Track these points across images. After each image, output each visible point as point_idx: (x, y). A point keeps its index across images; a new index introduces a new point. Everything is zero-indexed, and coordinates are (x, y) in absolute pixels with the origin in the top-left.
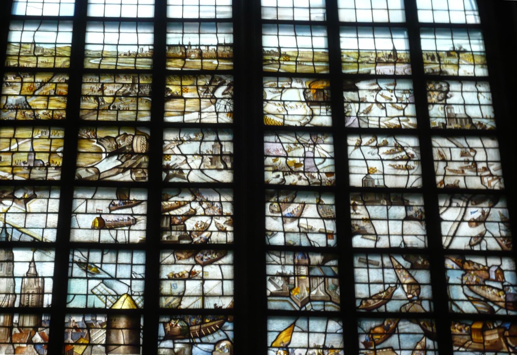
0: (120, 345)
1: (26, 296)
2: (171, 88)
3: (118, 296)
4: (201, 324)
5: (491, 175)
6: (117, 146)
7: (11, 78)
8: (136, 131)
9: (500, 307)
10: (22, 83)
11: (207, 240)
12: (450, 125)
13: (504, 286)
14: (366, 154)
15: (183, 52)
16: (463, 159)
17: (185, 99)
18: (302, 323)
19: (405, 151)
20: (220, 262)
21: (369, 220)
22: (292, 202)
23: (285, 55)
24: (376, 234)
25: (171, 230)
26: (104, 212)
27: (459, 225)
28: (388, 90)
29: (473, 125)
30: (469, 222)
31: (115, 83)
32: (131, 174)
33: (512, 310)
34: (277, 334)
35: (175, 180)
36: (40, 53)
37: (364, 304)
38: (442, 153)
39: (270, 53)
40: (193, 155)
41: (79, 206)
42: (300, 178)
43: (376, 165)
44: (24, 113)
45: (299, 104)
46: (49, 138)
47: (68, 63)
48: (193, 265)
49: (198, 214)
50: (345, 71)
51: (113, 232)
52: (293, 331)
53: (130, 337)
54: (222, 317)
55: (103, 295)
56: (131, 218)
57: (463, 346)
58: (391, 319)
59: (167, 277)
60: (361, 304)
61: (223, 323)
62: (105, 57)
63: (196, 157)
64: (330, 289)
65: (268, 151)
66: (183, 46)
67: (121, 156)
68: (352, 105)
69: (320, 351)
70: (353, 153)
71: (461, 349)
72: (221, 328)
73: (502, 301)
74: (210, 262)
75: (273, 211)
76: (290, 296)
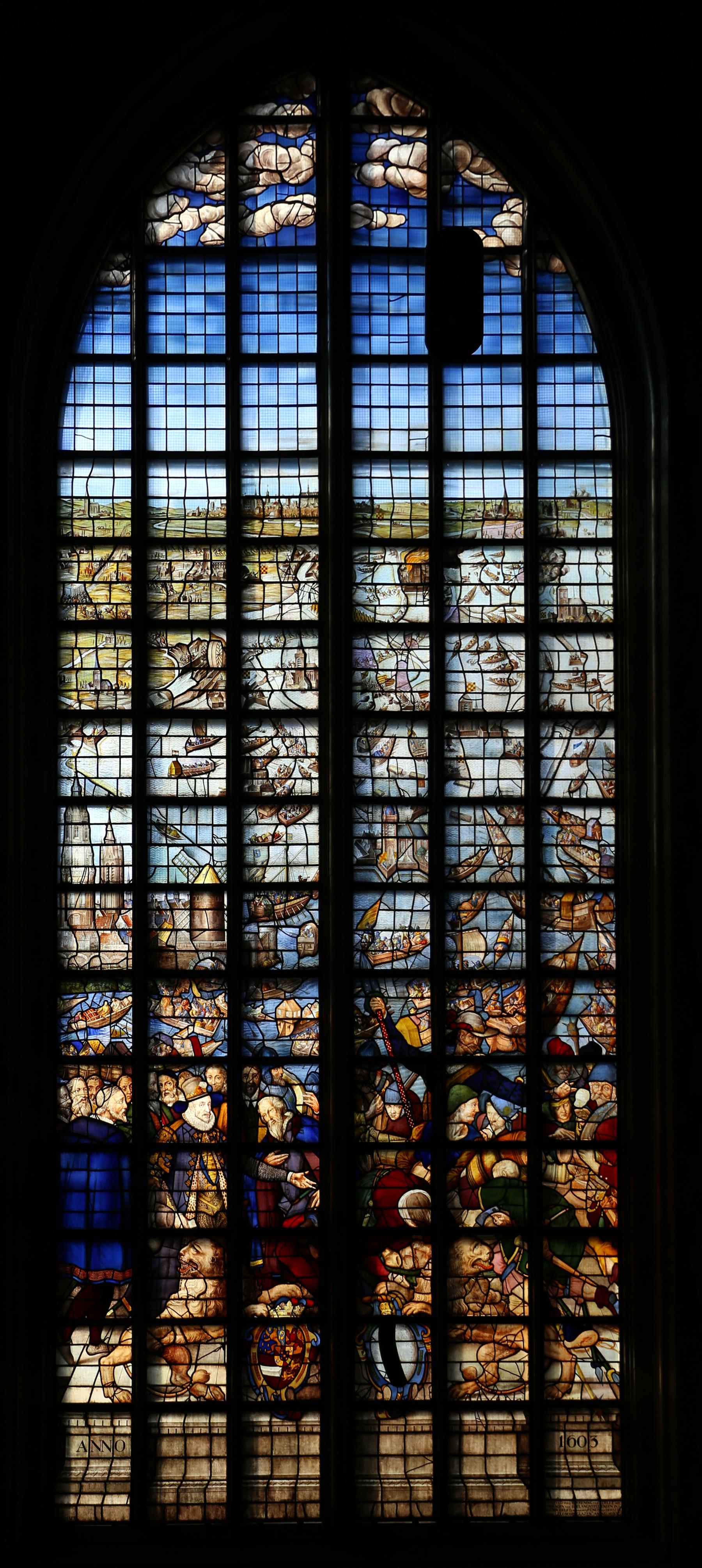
0: (205, 930)
2: (249, 567)
5: (601, 691)
6: (191, 657)
8: (211, 635)
10: (79, 562)
11: (291, 790)
12: (562, 617)
13: (600, 846)
14: (464, 662)
16: (571, 668)
17: (264, 583)
18: (388, 898)
20: (304, 821)
22: (382, 736)
24: (470, 779)
28: (495, 563)
29: (588, 615)
30: (570, 759)
31: (184, 560)
32: (207, 699)
33: (605, 878)
34: (362, 913)
36: (95, 515)
40: (274, 669)
42: (391, 702)
44: (85, 609)
45: (392, 588)
46: (115, 648)
47: (129, 529)
48: (277, 825)
51: (192, 781)
52: (379, 910)
53: (215, 920)
54: (306, 893)
55: (184, 866)
56: (210, 762)
61: (308, 901)
63: (278, 672)
66: (260, 497)
67: (195, 672)
68: (453, 588)
71: (549, 929)
72: (306, 907)
73: (596, 867)
74: (294, 823)
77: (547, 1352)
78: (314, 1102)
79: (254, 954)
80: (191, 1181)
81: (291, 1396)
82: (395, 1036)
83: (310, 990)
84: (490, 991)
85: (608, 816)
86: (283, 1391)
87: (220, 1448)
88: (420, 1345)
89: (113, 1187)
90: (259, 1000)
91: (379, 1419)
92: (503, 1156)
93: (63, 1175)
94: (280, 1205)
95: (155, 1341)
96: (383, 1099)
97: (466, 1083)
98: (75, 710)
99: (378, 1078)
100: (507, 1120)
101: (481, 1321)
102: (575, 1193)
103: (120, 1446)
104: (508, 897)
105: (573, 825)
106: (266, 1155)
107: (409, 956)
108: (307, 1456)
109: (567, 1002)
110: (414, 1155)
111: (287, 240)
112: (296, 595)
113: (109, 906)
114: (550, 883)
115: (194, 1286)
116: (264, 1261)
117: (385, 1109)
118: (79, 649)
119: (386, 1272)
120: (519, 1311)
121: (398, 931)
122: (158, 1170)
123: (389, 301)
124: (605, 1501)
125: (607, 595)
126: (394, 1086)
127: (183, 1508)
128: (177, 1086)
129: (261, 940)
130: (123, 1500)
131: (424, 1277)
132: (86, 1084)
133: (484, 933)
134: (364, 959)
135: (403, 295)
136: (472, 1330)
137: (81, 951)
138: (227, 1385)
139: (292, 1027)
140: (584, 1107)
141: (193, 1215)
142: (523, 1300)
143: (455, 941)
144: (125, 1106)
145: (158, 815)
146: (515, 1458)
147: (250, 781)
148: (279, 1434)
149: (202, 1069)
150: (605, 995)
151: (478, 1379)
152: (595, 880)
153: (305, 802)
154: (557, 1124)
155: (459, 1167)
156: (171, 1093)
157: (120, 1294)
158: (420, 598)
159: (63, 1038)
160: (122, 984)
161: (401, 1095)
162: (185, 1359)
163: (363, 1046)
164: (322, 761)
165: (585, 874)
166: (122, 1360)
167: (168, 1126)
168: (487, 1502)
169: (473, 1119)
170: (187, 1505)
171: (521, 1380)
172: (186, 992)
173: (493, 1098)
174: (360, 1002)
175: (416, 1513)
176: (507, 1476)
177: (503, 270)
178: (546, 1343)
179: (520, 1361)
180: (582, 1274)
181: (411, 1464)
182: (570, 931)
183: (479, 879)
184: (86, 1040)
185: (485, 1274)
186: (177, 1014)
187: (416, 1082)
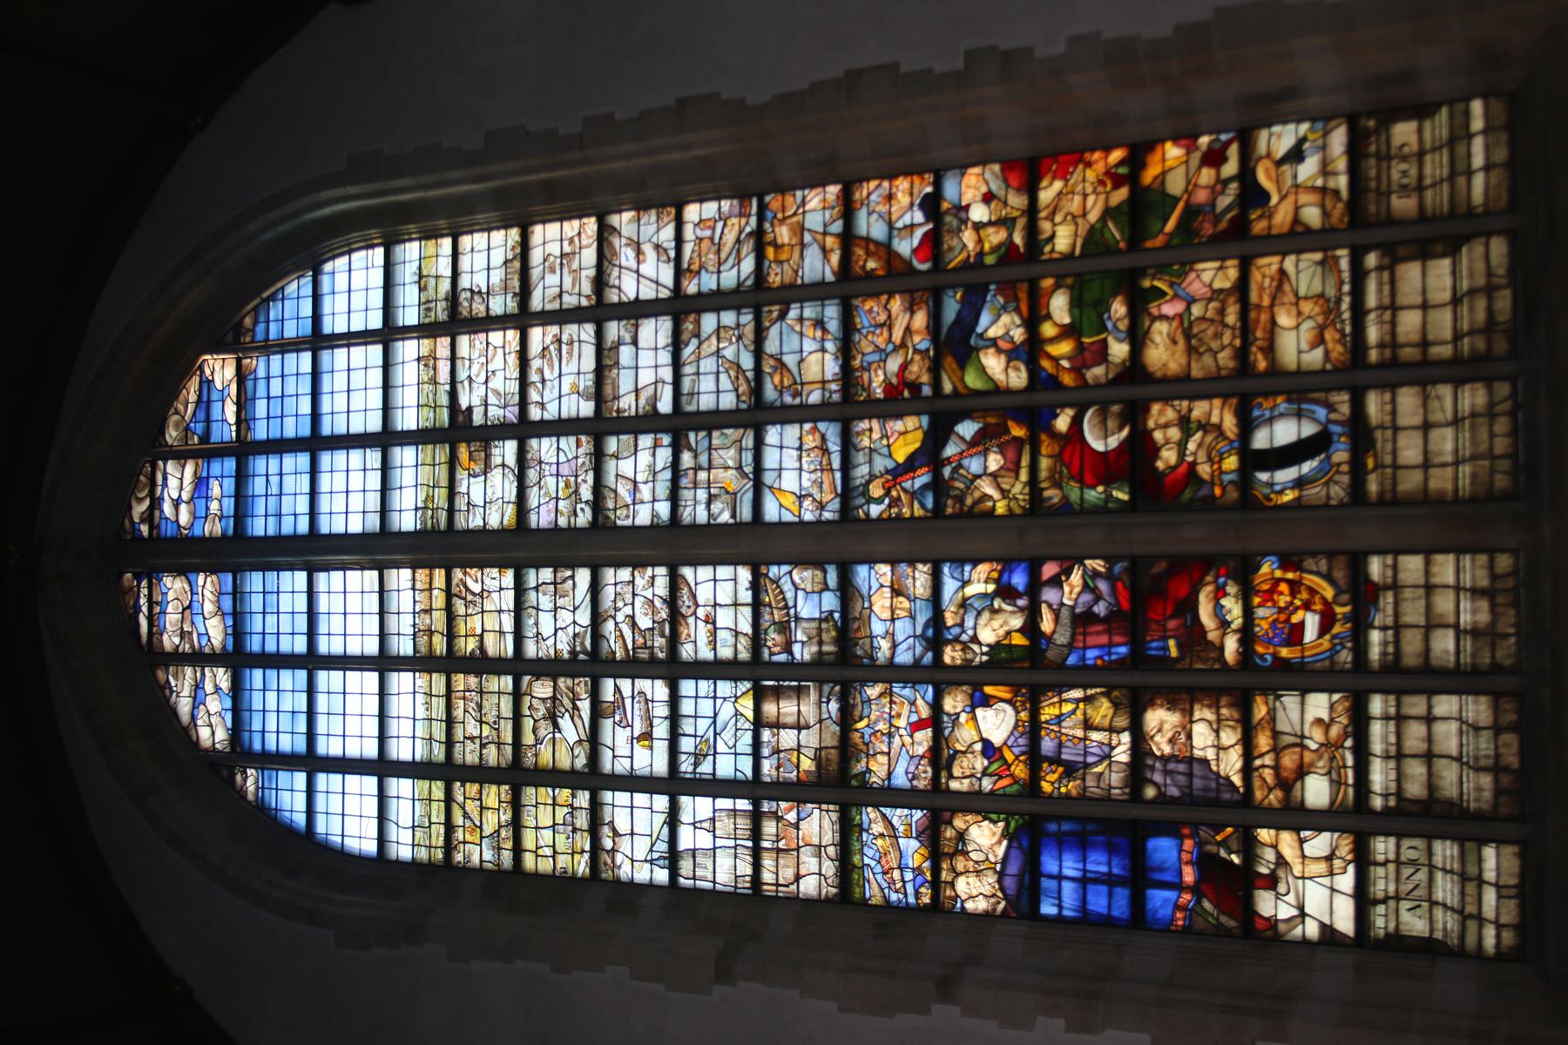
0: (799, 711)
1: (738, 832)
2: (469, 650)
3: (737, 714)
7: (458, 857)
9: (747, 223)
10: (465, 842)
11: (665, 601)
13: (720, 219)
16: (558, 271)
17: (483, 631)
18: (768, 478)
20: (692, 584)
21: (637, 391)
22: (615, 491)
23: (426, 501)
24: (656, 383)
25: (653, 647)
29: (514, 258)
30: (638, 263)
34: (783, 510)
35: (588, 643)
37: (744, 398)
39: (424, 522)
41: (622, 766)
42: (585, 481)
43: (567, 382)
48: (697, 618)
50: (447, 425)
51: (656, 722)
53: (789, 697)
57: (796, 272)
58: (764, 363)
68: (489, 414)
69: (804, 454)
70: (551, 413)
72: (776, 582)
74: (694, 596)
75: (628, 517)
76: (735, 494)
77: (1285, 229)
78: (983, 569)
79: (826, 648)
81: (1345, 597)
82: (910, 465)
84: (864, 343)
85: (692, 212)
87: (1415, 704)
88: (1276, 413)
89: (1081, 844)
90: (872, 642)
91: (1376, 467)
92: (1044, 313)
93: (1066, 913)
94: (1102, 615)
95: (1271, 797)
96: (979, 476)
97: (962, 366)
98: (591, 858)
100: (1004, 308)
101: (1246, 329)
103: (1413, 854)
104: (768, 328)
105: (700, 255)
106: (1043, 633)
108: (1427, 573)
109: (877, 243)
111: (227, 603)
113: (774, 831)
115: (1202, 737)
116: (1170, 637)
120: (1233, 274)
125: (498, 236)
126: (966, 462)
127: (1503, 762)
128: (964, 753)
129: (810, 638)
130: (1489, 853)
131: (1190, 410)
132: (962, 873)
133: (805, 354)
134: (830, 507)
135: (267, 480)
136: (1256, 339)
137: (820, 869)
138: (1331, 691)
139: (901, 599)
141: (1114, 735)
142: (1221, 268)
143: (811, 392)
144: (986, 822)
147: (656, 650)
148: (1396, 615)
150: (869, 194)
152: (753, 221)
153: (675, 582)
154: (1009, 244)
157: (1211, 843)
159: (911, 900)
162: (1295, 753)
163: (923, 506)
164: (637, 564)
166: (1296, 845)
168: (1490, 300)
170: (1497, 756)
172: (862, 737)
173: (979, 330)
174: (875, 510)
175: (1506, 406)
176: (1454, 273)
177: (252, 376)
178: (1274, 231)
179: (1297, 266)
180: (1186, 190)
181: (1437, 416)
182: (803, 246)
184: (913, 870)
186: (886, 750)
187: (961, 433)
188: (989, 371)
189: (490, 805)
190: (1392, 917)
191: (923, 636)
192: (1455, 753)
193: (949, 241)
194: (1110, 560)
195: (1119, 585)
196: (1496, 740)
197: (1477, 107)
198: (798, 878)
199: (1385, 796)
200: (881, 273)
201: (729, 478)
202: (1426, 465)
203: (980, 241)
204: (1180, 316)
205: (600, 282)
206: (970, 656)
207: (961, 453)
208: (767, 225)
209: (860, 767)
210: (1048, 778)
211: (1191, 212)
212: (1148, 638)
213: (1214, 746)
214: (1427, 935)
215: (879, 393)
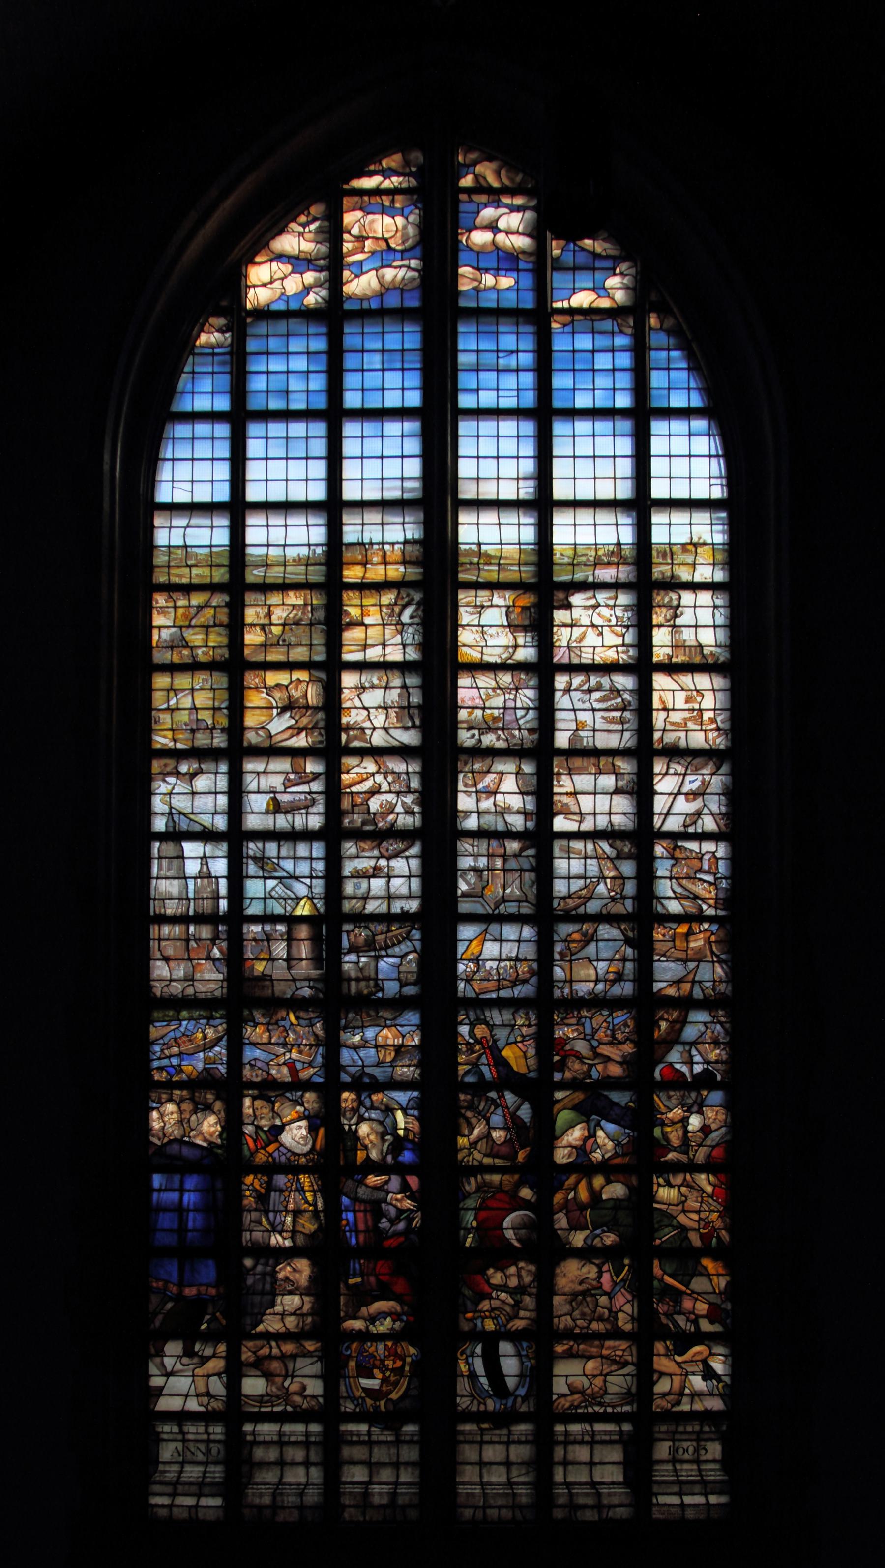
0: (302, 960)
1: (201, 901)
3: (299, 899)
4: (386, 933)
6: (290, 697)
7: (160, 600)
10: (175, 607)
11: (393, 825)
12: (677, 657)
13: (716, 879)
14: (575, 701)
15: (363, 555)
16: (687, 706)
17: (366, 626)
18: (494, 928)
19: (621, 696)
20: (407, 854)
22: (488, 772)
23: (487, 555)
24: (581, 814)
25: (353, 813)
26: (278, 790)
27: (674, 799)
28: (607, 606)
29: (704, 656)
30: (686, 794)
31: (283, 604)
32: (307, 737)
34: (467, 943)
35: (356, 744)
37: (562, 904)
38: (664, 699)
40: (376, 708)
41: (251, 783)
42: (498, 739)
44: (181, 652)
45: (502, 629)
47: (227, 576)
48: (378, 858)
49: (383, 790)
50: (555, 579)
51: (289, 817)
52: (485, 940)
53: (313, 951)
55: (282, 898)
56: (309, 797)
57: (664, 955)
58: (590, 924)
59: (349, 874)
60: (559, 904)
61: (410, 932)
62: (271, 565)
63: (380, 710)
64: (527, 886)
65: (463, 701)
66: (363, 544)
67: (294, 711)
68: (563, 629)
69: (512, 963)
70: (562, 701)
71: (662, 959)
72: (408, 937)
74: (396, 855)
75: (466, 785)
76: (482, 896)
77: (656, 1366)
78: (415, 1126)
79: (353, 984)
80: (288, 1202)
81: (391, 1407)
82: (500, 1062)
83: (412, 1018)
84: (600, 1019)
86: (382, 1403)
88: (524, 1359)
89: (206, 1208)
90: (358, 1028)
91: (482, 1430)
92: (612, 1178)
93: (155, 1196)
94: (380, 1225)
95: (250, 1354)
96: (488, 1123)
97: (575, 1108)
99: (483, 1104)
100: (618, 1144)
102: (688, 1214)
103: (214, 1451)
104: (619, 928)
105: (688, 858)
106: (366, 1177)
107: (516, 985)
109: (681, 1030)
110: (520, 1178)
111: (392, 302)
112: (399, 636)
113: (204, 936)
114: (662, 915)
115: (292, 1302)
116: (363, 1279)
117: (489, 1133)
118: (175, 690)
119: (490, 1290)
120: (628, 1327)
121: (505, 960)
122: (253, 1191)
123: (498, 357)
124: (714, 1505)
126: (499, 1111)
128: (273, 1109)
129: (361, 970)
130: (217, 1502)
131: (530, 1295)
132: (179, 1108)
133: (595, 963)
134: (468, 988)
135: (512, 352)
136: (578, 1345)
137: (175, 980)
139: (393, 1054)
140: (698, 1131)
141: (289, 1234)
143: (564, 970)
144: (219, 1128)
145: (255, 848)
146: (622, 1466)
148: (379, 1443)
149: (299, 1093)
150: (721, 1023)
151: (584, 1391)
152: (711, 912)
153: (407, 836)
154: (669, 1148)
155: (567, 1189)
156: (267, 1117)
158: (529, 639)
159: (156, 1064)
160: (216, 1012)
161: (506, 1120)
162: (281, 1371)
163: (467, 1073)
165: (700, 906)
166: (216, 1371)
167: (264, 1148)
168: (592, 1507)
169: (581, 1143)
170: (283, 1508)
171: (629, 1392)
172: (283, 1019)
173: (603, 1123)
174: (464, 1030)
175: (519, 1516)
176: (613, 1483)
177: (616, 329)
179: (628, 1375)
180: (693, 1292)
181: (515, 1472)
182: (685, 961)
183: (589, 911)
184: (180, 1065)
185: (593, 1292)
186: (273, 1041)
187: (522, 1107)
188: (570, 1131)
189: (212, 637)
190: (171, 1437)
191: (364, 1074)
192: (284, 1480)
193: (676, 1095)
194: (420, 1231)
195: (402, 1239)
196: (294, 1507)
197: (723, 1499)
198: (166, 959)
199: (253, 1433)
200: (656, 1035)
201: (495, 891)
202: (482, 1464)
203: (673, 1123)
204: (600, 1287)
205: (673, 753)
206: (348, 1115)
207: (507, 1107)
208: (706, 926)
209: (258, 1016)
210: (256, 1180)
211: (676, 1296)
212: (362, 1261)
213: (284, 1311)
214: (160, 1460)
215: (559, 1033)
